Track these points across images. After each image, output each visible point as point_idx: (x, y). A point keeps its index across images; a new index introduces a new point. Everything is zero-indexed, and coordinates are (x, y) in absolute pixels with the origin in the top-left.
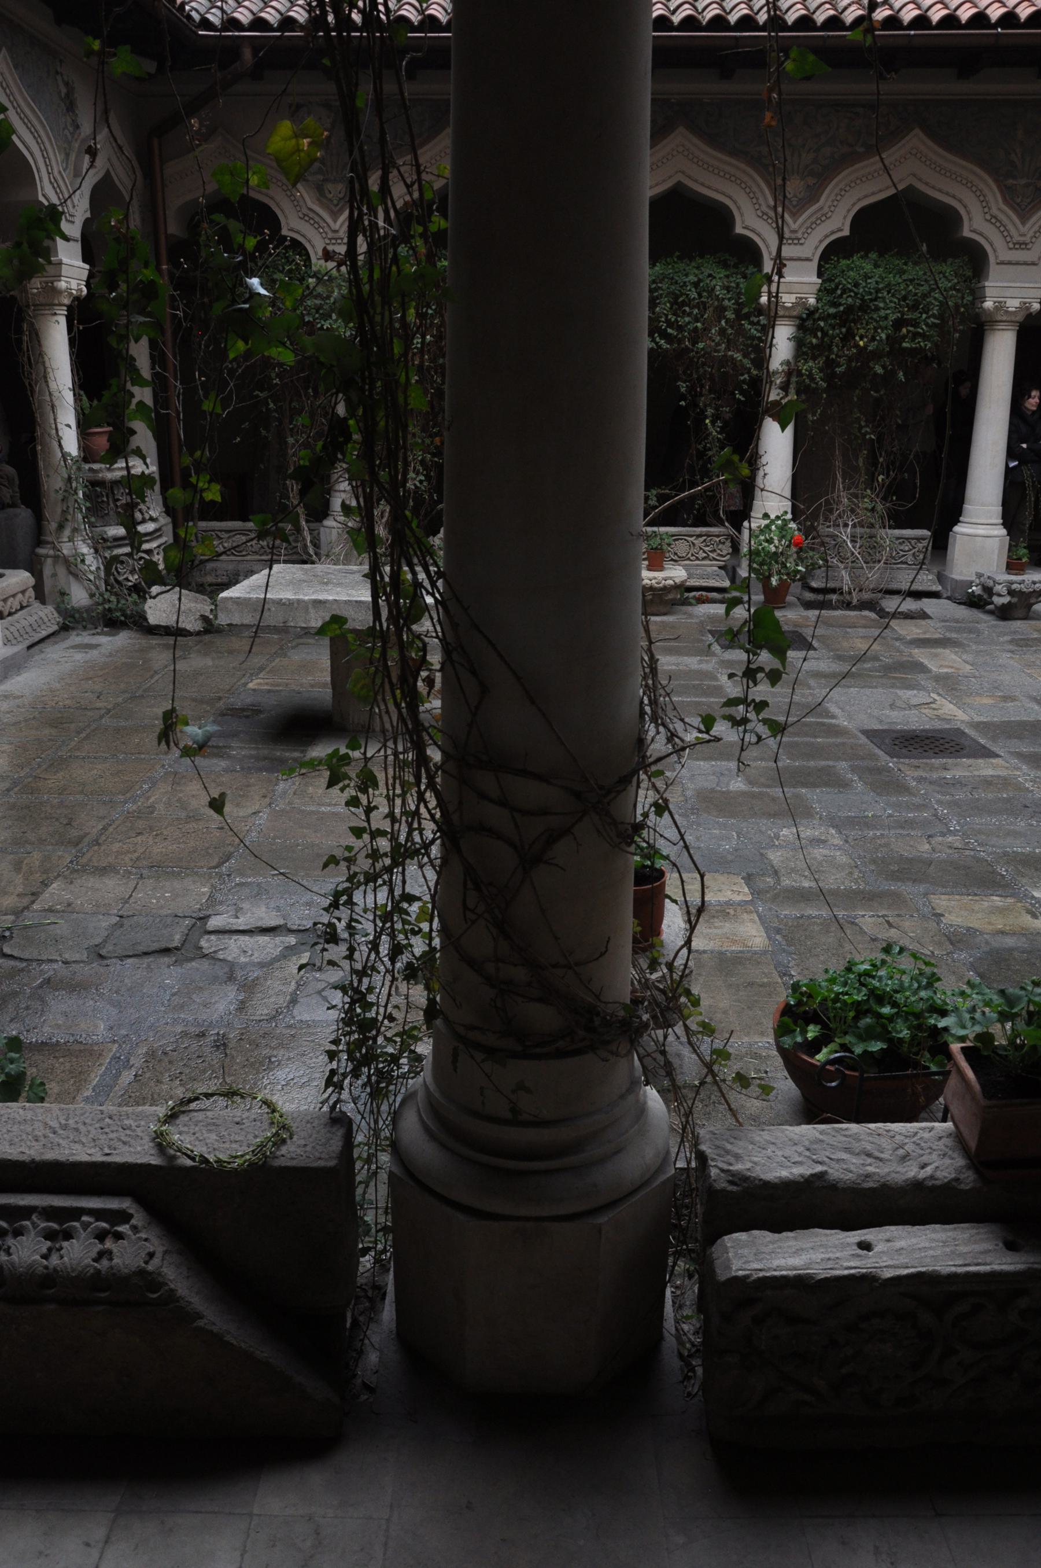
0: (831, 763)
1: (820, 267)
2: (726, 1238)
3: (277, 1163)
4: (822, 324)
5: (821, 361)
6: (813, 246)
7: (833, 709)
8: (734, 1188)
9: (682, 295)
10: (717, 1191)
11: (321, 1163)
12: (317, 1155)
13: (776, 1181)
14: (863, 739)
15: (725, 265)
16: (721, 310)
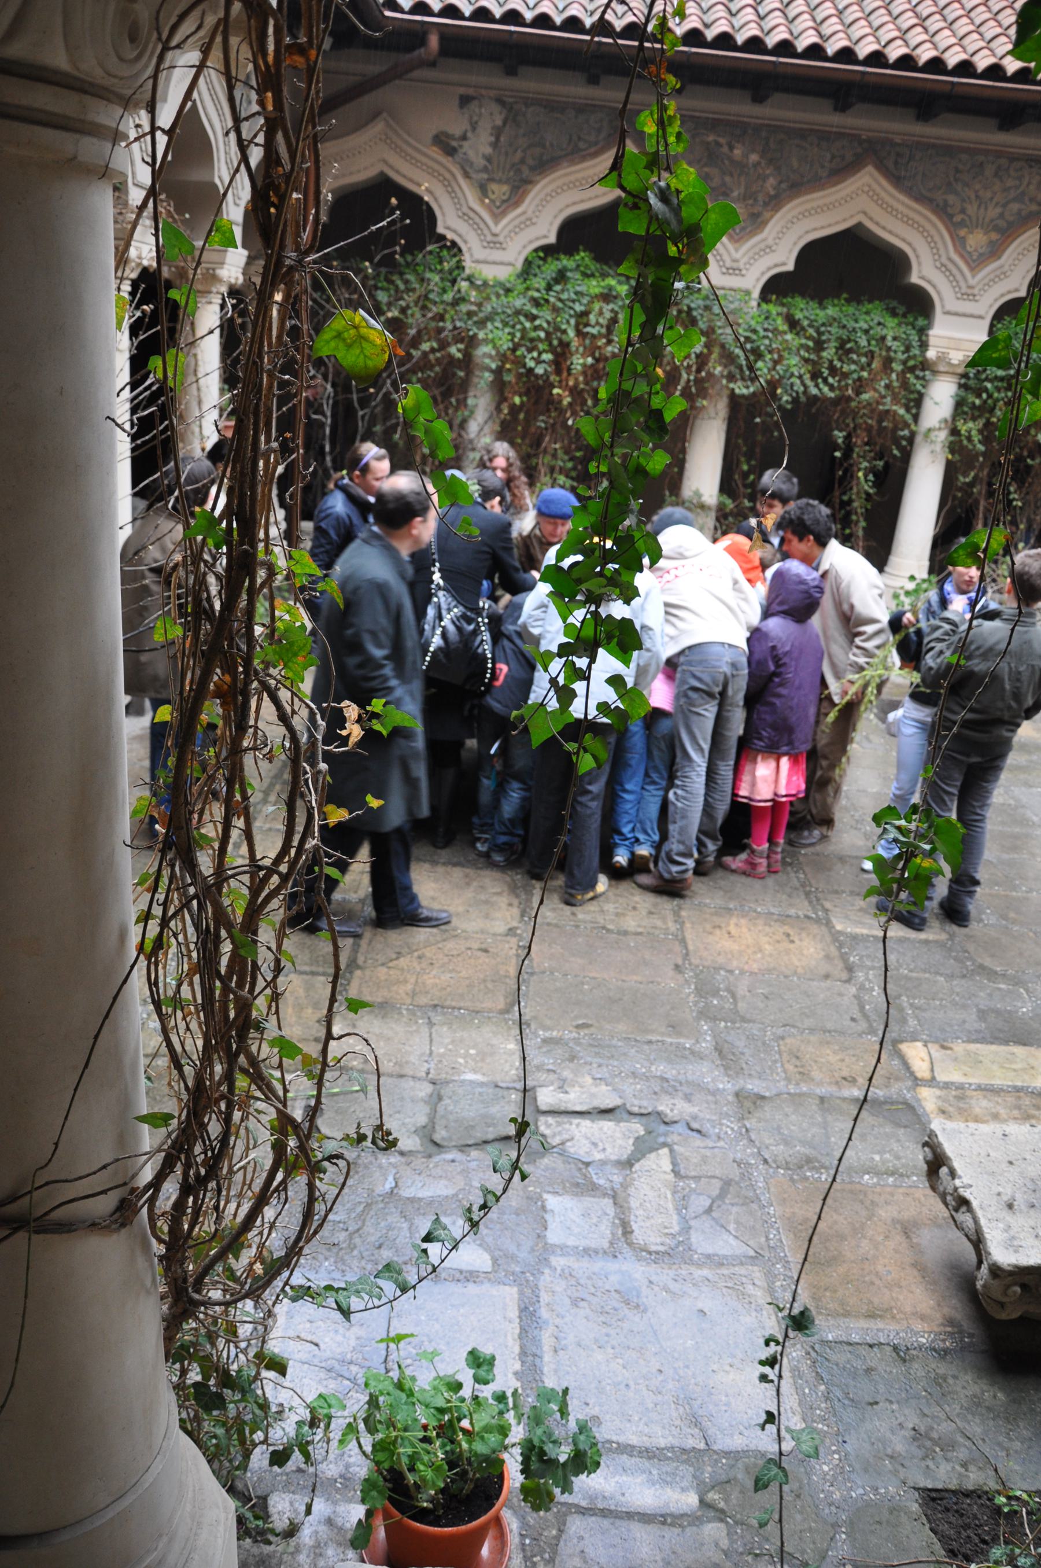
1: (992, 326)
4: (989, 385)
5: (981, 423)
6: (988, 304)
9: (849, 340)
15: (894, 314)
16: (888, 362)
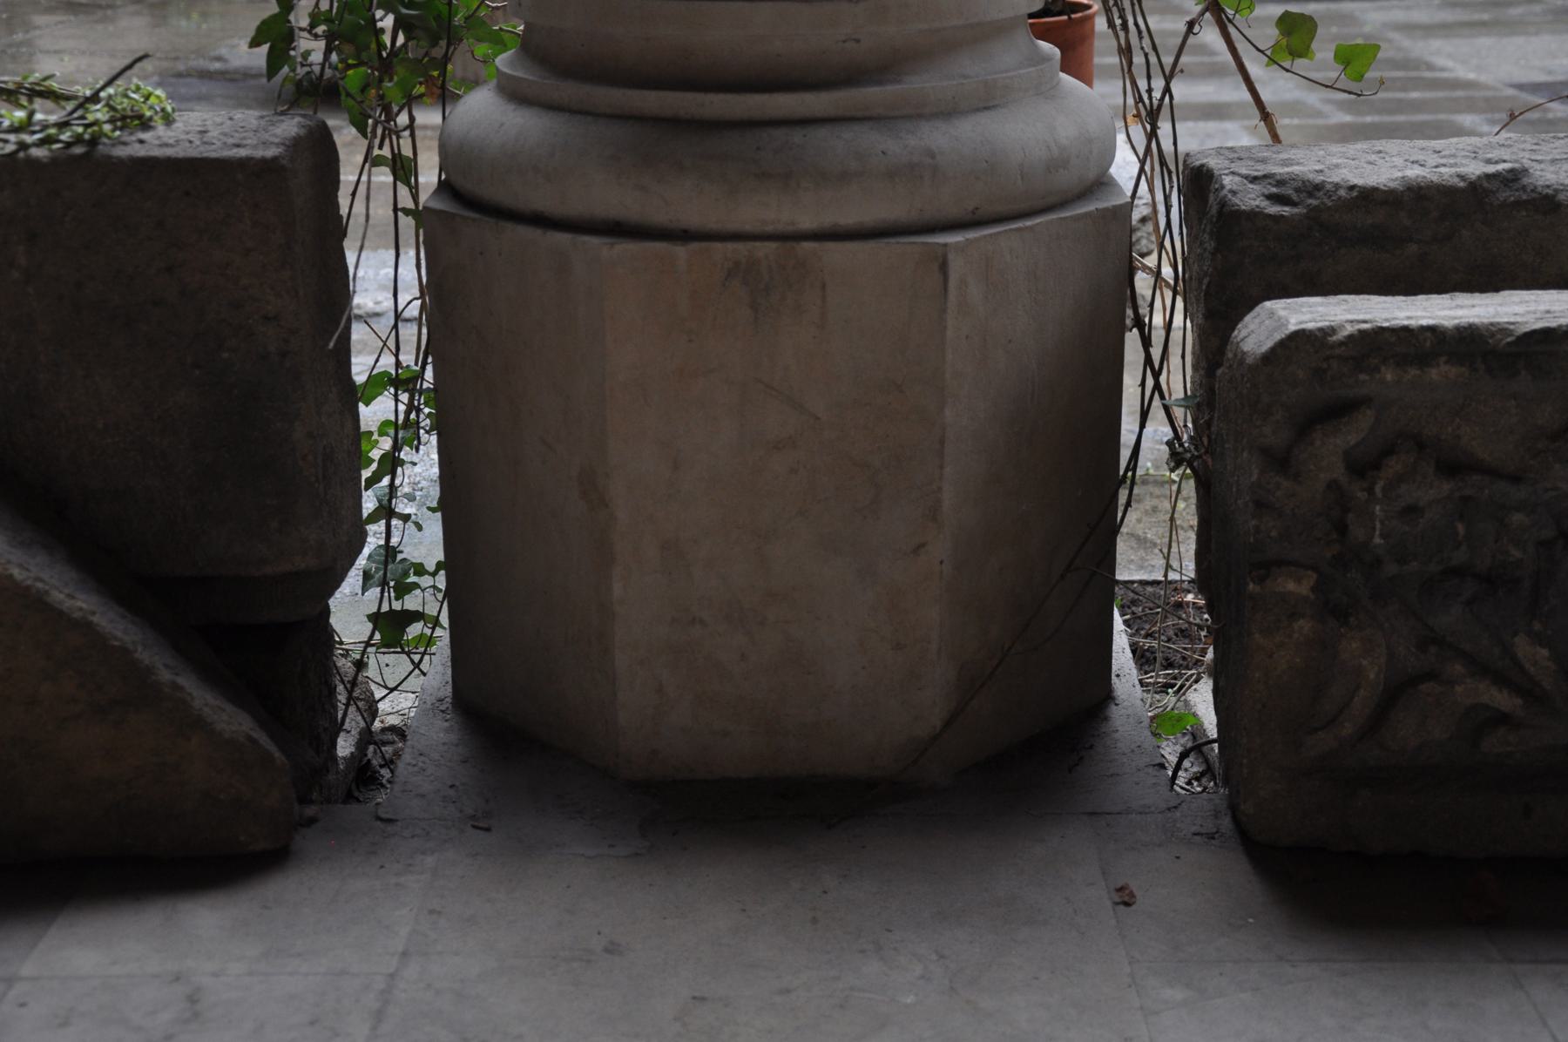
0: (1442, 117)
2: (1268, 304)
3: (121, 152)
7: (1440, 61)
8: (1286, 210)
10: (1239, 215)
11: (243, 153)
12: (231, 141)
13: (1392, 185)
14: (1511, 92)
